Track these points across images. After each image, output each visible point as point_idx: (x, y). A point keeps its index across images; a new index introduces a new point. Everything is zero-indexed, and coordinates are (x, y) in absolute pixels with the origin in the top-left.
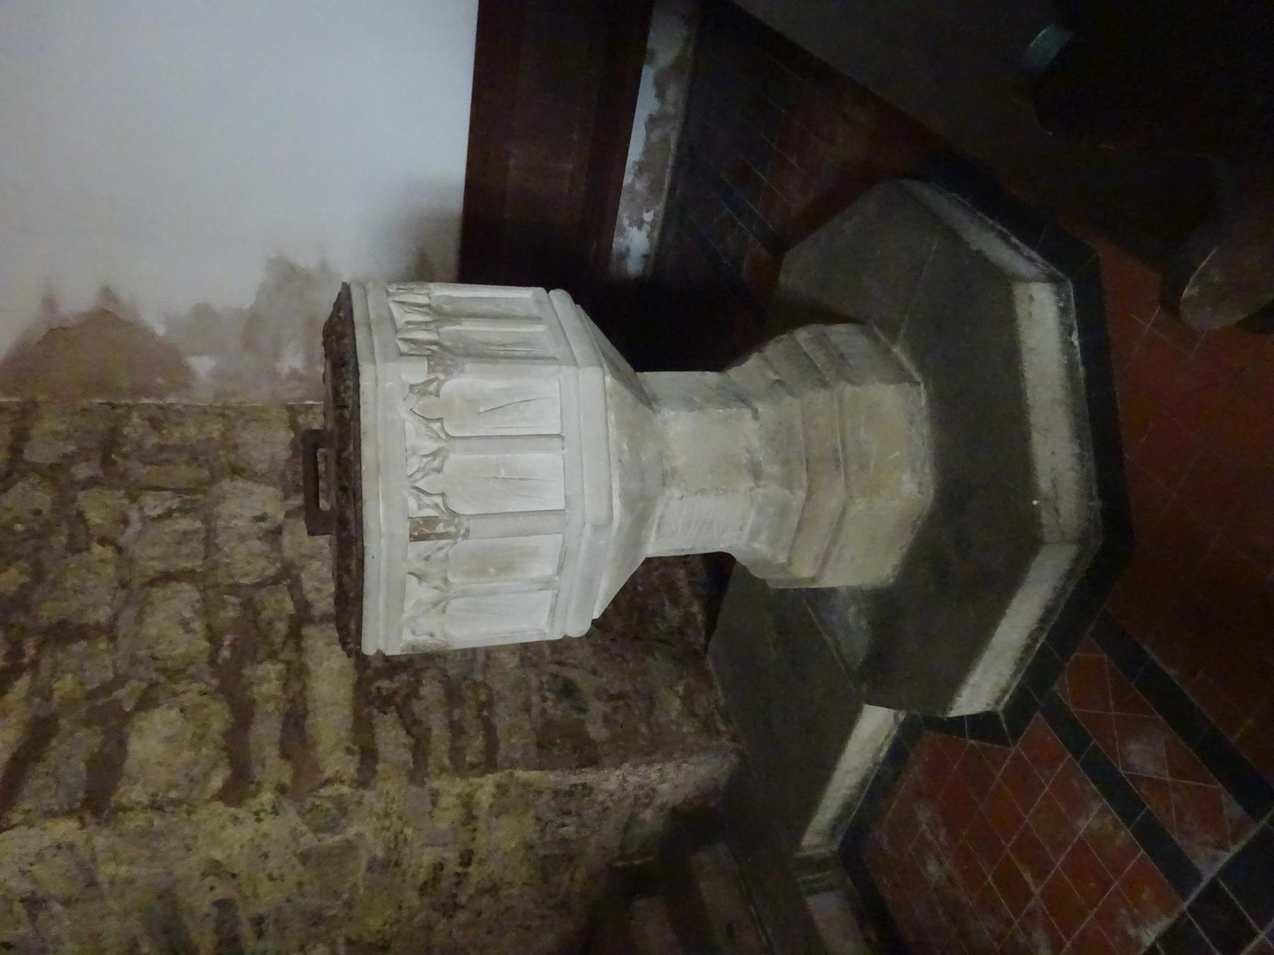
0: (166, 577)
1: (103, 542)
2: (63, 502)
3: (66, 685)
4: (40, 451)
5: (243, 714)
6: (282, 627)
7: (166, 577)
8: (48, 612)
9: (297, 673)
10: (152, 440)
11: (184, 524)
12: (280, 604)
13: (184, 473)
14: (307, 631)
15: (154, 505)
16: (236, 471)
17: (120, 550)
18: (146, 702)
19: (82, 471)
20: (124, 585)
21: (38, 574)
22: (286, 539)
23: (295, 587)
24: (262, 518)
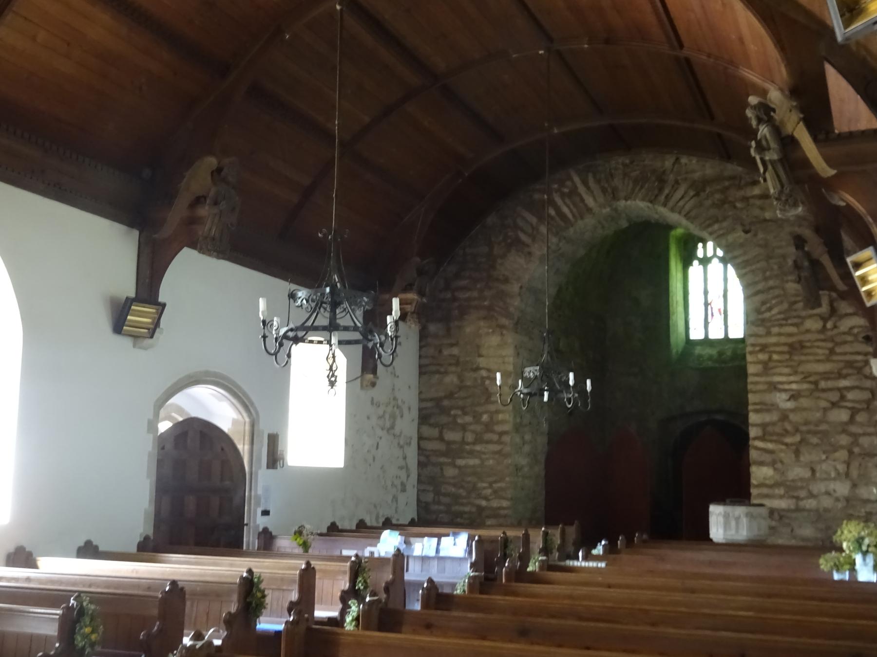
0: (813, 471)
1: (827, 458)
2: (842, 447)
3: (782, 455)
4: (865, 441)
5: (771, 487)
6: (795, 494)
7: (813, 471)
8: (803, 449)
9: (781, 497)
10: (870, 465)
11: (833, 475)
12: (803, 494)
13: (854, 473)
14: (794, 501)
15: (841, 468)
16: (854, 486)
17: (824, 461)
18: (775, 469)
19: (856, 450)
20: (812, 462)
21: (817, 445)
22: (825, 497)
23: (808, 498)
24: (835, 491)
